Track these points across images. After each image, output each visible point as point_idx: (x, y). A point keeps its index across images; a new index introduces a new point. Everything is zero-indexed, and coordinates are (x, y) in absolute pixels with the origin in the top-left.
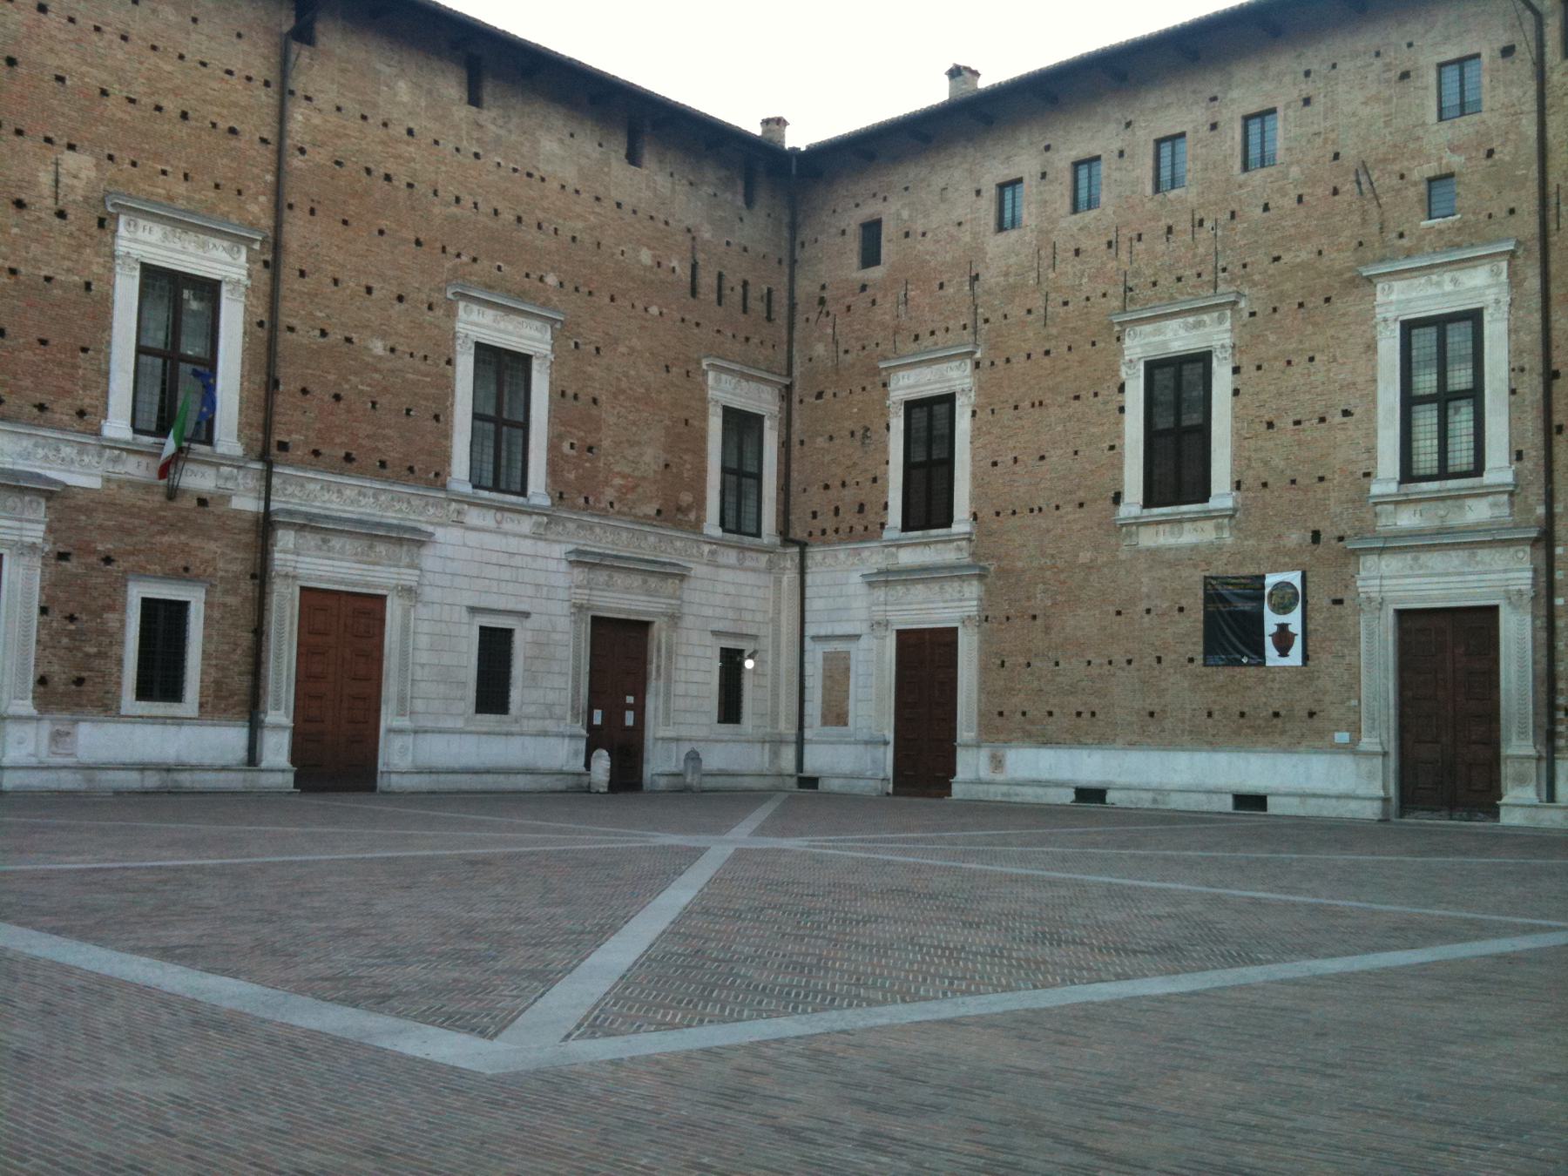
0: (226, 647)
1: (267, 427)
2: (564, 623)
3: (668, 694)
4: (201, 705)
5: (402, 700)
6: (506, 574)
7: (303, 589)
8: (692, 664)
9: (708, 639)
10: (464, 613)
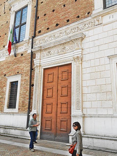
0: (25, 91)
1: (35, 30)
4: (19, 109)
5: (78, 102)
7: (44, 69)
10: (107, 59)
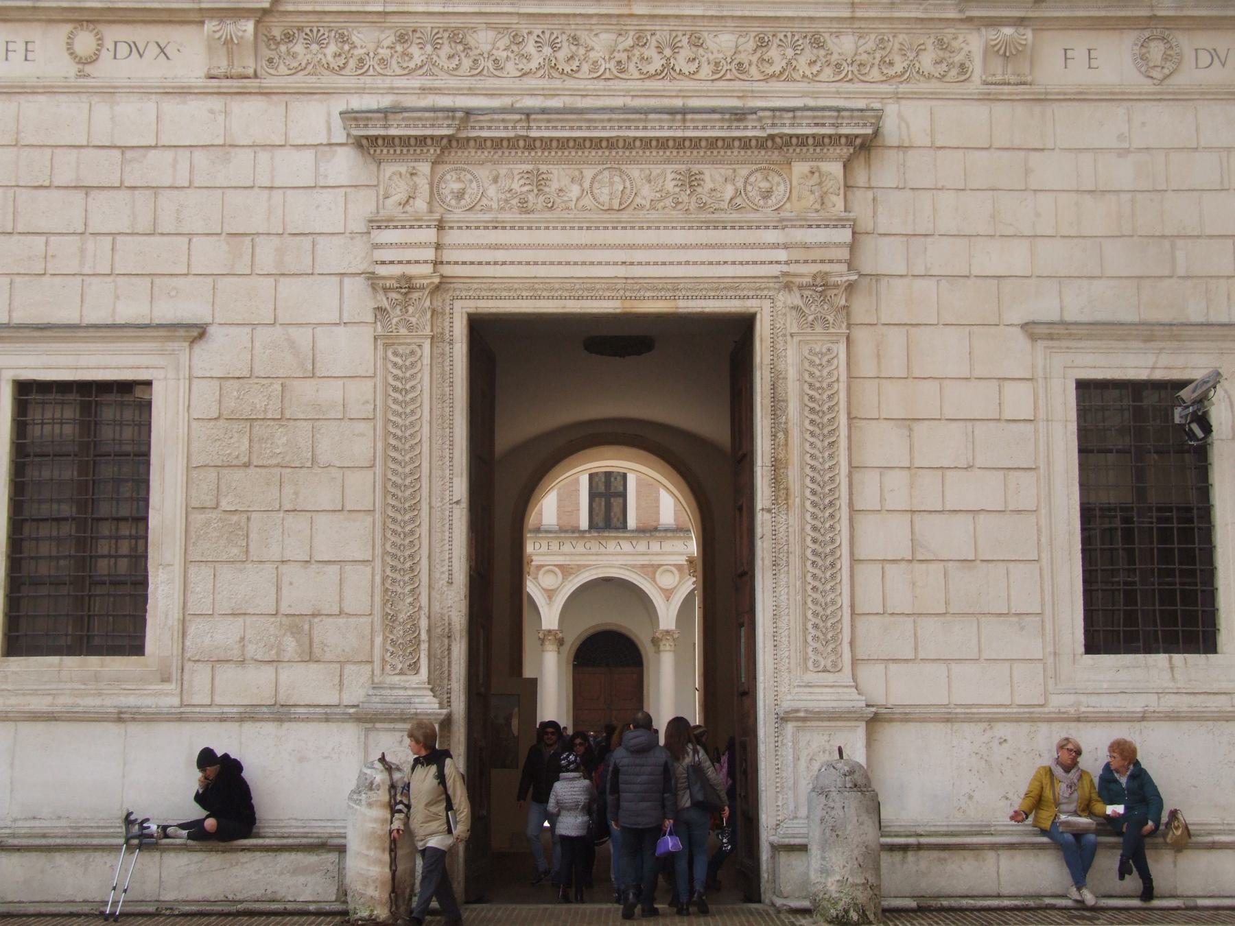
2: (351, 349)
3: (823, 559)
6: (109, 212)
8: (940, 445)
9: (1018, 356)
